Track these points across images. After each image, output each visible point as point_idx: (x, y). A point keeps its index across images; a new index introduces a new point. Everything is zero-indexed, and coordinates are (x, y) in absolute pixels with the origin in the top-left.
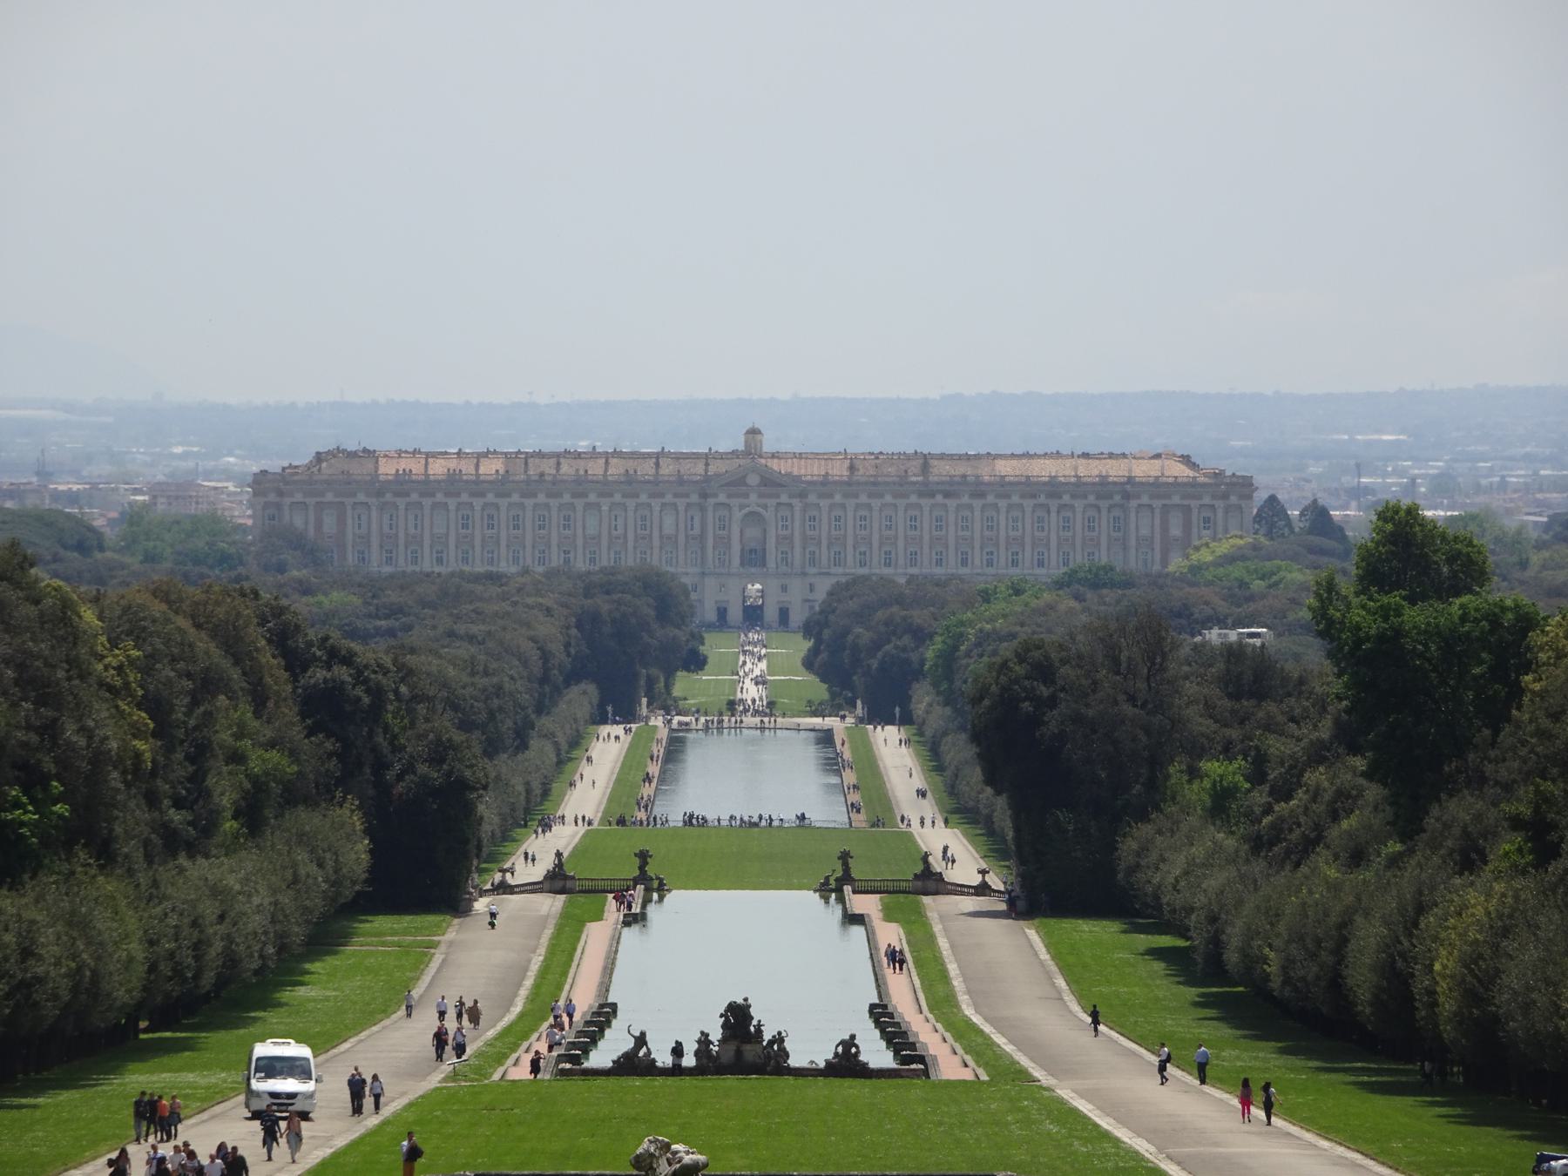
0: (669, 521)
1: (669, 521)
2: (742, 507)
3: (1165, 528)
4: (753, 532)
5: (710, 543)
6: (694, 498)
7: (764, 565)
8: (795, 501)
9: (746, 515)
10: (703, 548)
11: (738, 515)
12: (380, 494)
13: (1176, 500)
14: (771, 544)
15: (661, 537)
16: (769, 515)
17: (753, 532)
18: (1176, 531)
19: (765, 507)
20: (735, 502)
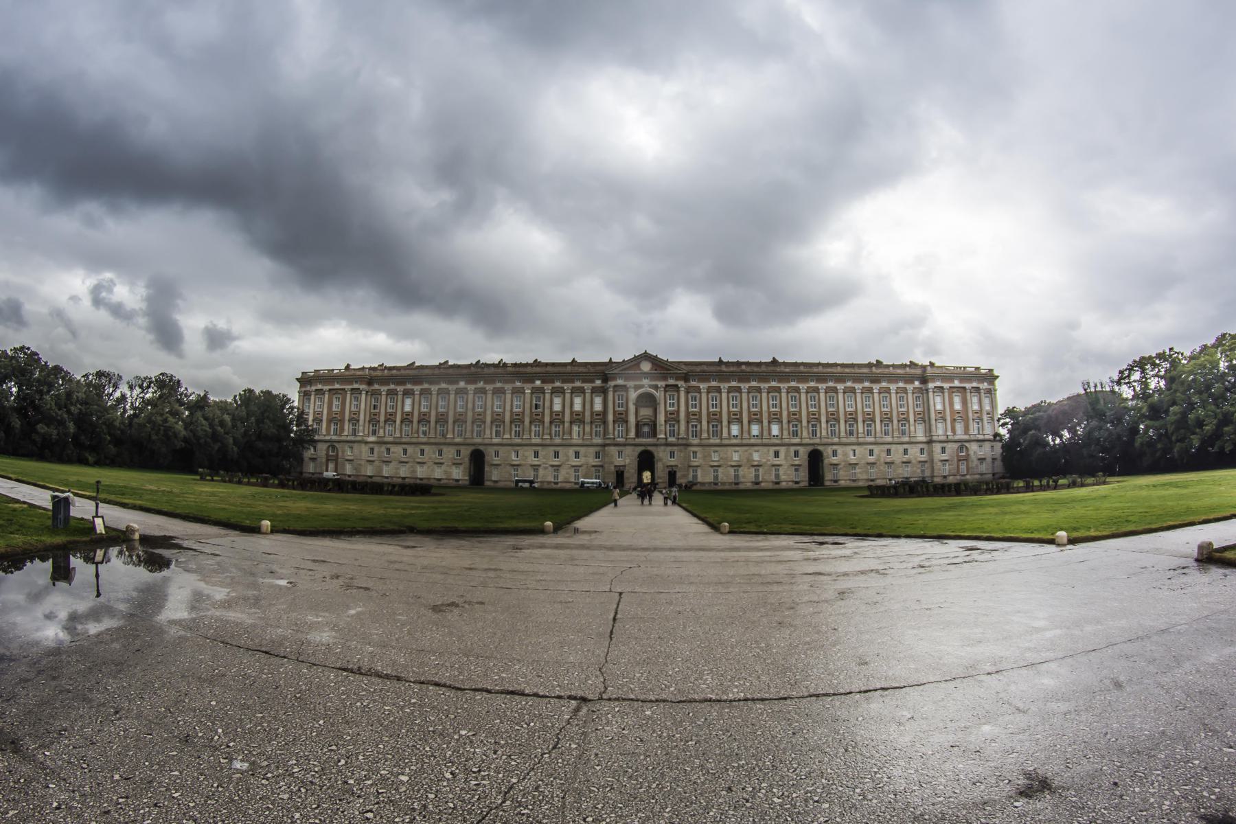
0: (578, 402)
1: (578, 402)
2: (637, 387)
3: (951, 404)
4: (646, 412)
5: (610, 417)
6: (598, 382)
7: (654, 433)
8: (680, 383)
9: (641, 397)
10: (605, 422)
11: (633, 395)
12: (370, 382)
13: (956, 383)
14: (661, 418)
15: (572, 413)
16: (659, 395)
17: (646, 412)
18: (958, 407)
19: (656, 387)
20: (631, 384)
